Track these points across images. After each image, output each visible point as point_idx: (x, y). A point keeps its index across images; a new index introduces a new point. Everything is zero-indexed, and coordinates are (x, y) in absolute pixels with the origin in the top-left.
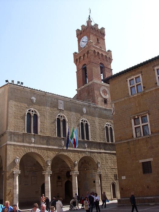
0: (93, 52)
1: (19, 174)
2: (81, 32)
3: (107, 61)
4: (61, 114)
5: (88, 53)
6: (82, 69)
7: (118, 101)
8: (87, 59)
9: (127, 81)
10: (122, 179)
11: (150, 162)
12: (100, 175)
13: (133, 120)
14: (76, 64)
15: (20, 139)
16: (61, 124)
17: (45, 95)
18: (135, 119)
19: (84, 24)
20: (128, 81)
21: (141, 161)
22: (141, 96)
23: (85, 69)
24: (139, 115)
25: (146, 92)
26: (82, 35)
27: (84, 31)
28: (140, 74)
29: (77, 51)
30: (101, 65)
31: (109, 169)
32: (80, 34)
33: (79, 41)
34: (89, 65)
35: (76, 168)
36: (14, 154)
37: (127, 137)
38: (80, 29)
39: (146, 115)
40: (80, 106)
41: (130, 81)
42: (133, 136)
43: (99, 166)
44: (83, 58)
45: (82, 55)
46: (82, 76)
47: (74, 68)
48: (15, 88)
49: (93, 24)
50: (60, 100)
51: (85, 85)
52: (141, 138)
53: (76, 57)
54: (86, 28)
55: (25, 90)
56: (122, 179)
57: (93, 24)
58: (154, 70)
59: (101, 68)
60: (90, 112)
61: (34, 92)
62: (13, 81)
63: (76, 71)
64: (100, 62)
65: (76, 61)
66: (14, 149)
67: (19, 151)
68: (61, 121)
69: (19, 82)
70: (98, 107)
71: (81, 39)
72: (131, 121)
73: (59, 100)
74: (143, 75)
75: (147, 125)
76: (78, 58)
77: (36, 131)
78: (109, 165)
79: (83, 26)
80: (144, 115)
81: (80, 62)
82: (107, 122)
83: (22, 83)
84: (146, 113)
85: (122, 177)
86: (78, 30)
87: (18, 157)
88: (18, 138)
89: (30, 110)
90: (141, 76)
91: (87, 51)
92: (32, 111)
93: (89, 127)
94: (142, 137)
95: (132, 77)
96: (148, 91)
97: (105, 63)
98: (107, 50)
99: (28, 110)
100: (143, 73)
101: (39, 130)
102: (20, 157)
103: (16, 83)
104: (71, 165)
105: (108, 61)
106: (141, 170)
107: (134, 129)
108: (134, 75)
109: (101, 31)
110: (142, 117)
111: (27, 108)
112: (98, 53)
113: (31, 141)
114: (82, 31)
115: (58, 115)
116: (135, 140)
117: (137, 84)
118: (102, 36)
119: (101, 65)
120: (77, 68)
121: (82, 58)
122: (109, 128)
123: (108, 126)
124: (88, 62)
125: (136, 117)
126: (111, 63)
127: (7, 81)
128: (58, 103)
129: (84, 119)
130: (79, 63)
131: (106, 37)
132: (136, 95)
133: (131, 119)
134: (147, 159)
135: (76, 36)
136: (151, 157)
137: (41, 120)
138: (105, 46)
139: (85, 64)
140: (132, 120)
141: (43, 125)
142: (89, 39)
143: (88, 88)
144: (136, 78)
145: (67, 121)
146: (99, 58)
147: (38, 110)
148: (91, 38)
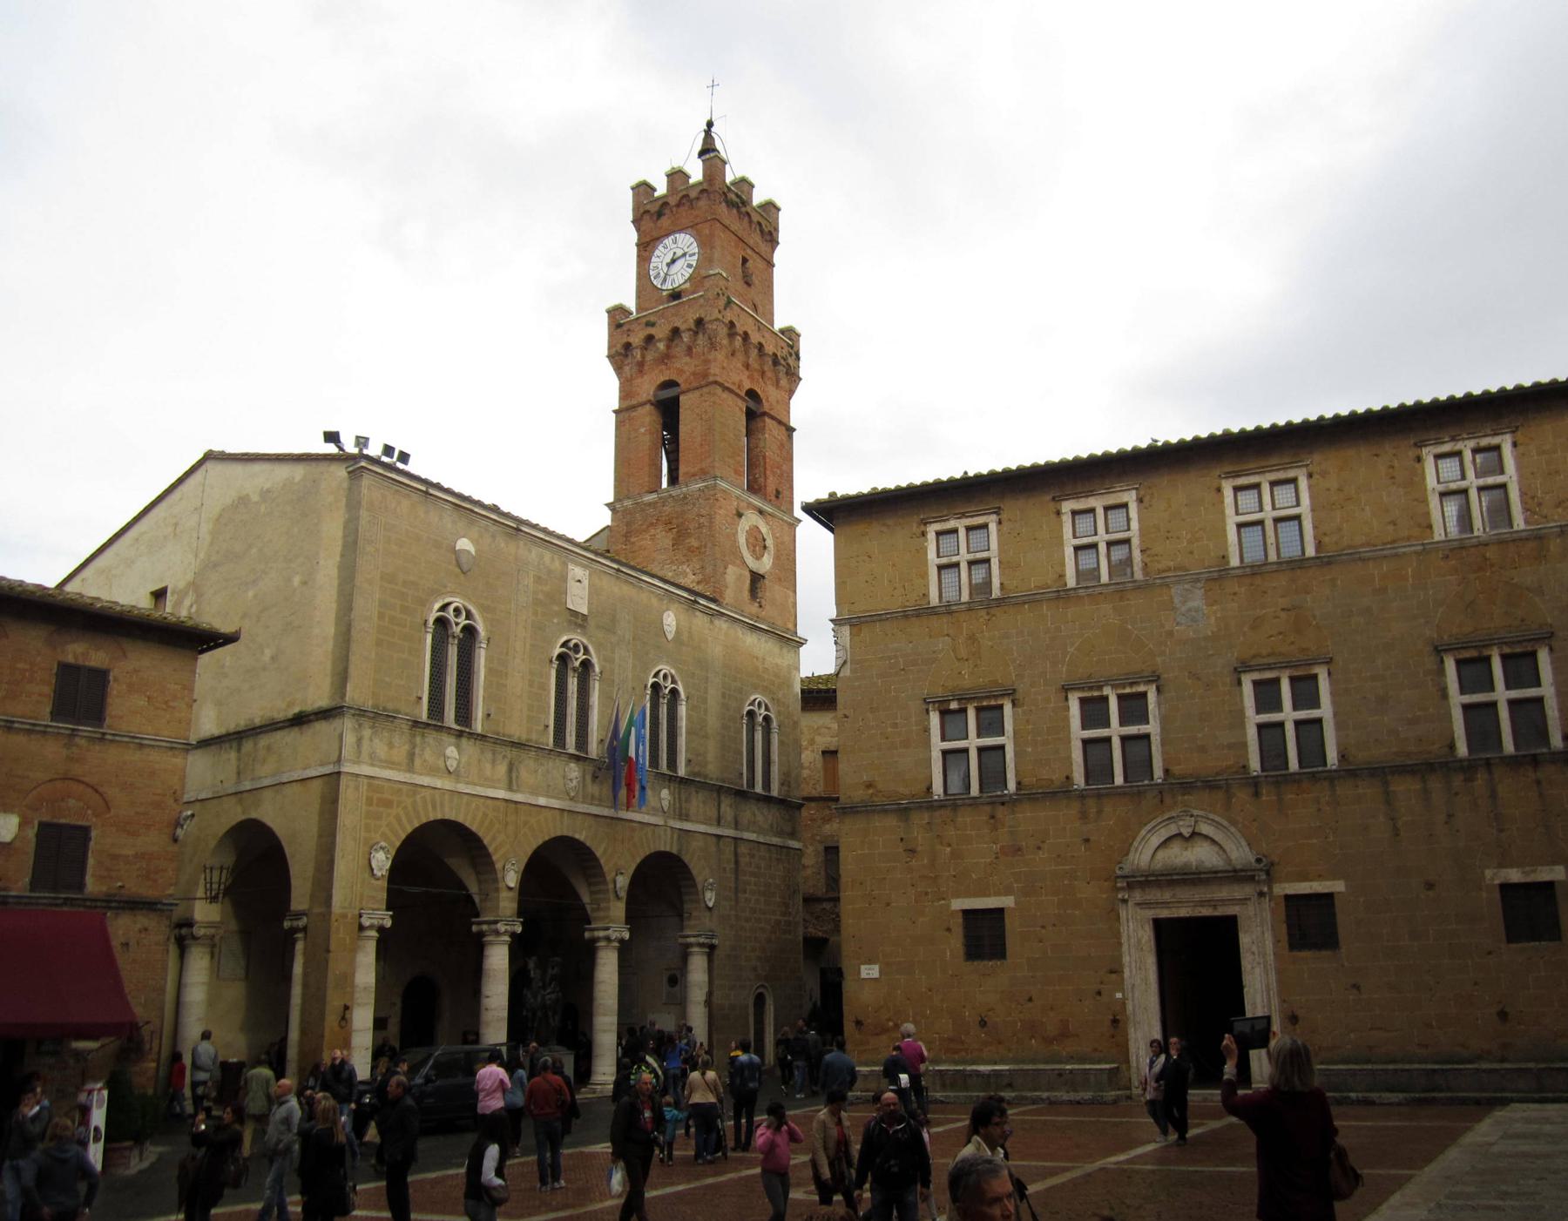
0: (723, 331)
1: (381, 929)
2: (666, 204)
3: (778, 381)
4: (576, 638)
9: (924, 534)
10: (864, 975)
11: (1000, 911)
12: (712, 947)
13: (935, 719)
14: (618, 369)
16: (573, 684)
18: (944, 713)
19: (687, 169)
20: (931, 536)
21: (959, 904)
23: (668, 411)
26: (665, 222)
27: (678, 205)
28: (994, 517)
29: (631, 304)
30: (752, 405)
31: (747, 920)
32: (656, 214)
33: (646, 248)
34: (697, 393)
35: (618, 909)
38: (661, 188)
40: (655, 601)
41: (939, 534)
42: (929, 788)
44: (668, 347)
45: (661, 332)
46: (647, 438)
47: (606, 388)
49: (729, 178)
50: (577, 564)
54: (693, 194)
56: (864, 975)
57: (729, 178)
59: (751, 415)
62: (362, 442)
63: (616, 407)
64: (747, 385)
65: (620, 355)
66: (369, 801)
68: (570, 674)
69: (388, 450)
71: (658, 239)
72: (928, 720)
73: (571, 566)
74: (1005, 523)
76: (637, 339)
77: (464, 714)
79: (676, 176)
80: (993, 703)
82: (756, 688)
83: (404, 457)
86: (643, 190)
87: (383, 844)
88: (391, 745)
89: (448, 604)
90: (993, 527)
91: (692, 316)
92: (457, 610)
93: (682, 710)
95: (951, 524)
98: (779, 323)
99: (437, 606)
100: (1004, 516)
101: (479, 712)
102: (391, 844)
103: (374, 450)
105: (784, 382)
106: (955, 943)
107: (936, 757)
108: (963, 515)
109: (764, 223)
112: (746, 336)
113: (442, 765)
114: (673, 201)
117: (971, 557)
118: (763, 247)
119: (752, 405)
121: (661, 346)
122: (760, 719)
123: (756, 708)
124: (694, 374)
125: (954, 706)
126: (791, 393)
127: (332, 437)
128: (564, 578)
129: (666, 669)
131: (778, 256)
133: (927, 711)
135: (630, 217)
136: (1007, 892)
137: (489, 659)
138: (771, 302)
139: (670, 384)
142: (706, 259)
143: (678, 509)
144: (969, 529)
145: (597, 669)
146: (747, 366)
147: (484, 609)
148: (717, 255)
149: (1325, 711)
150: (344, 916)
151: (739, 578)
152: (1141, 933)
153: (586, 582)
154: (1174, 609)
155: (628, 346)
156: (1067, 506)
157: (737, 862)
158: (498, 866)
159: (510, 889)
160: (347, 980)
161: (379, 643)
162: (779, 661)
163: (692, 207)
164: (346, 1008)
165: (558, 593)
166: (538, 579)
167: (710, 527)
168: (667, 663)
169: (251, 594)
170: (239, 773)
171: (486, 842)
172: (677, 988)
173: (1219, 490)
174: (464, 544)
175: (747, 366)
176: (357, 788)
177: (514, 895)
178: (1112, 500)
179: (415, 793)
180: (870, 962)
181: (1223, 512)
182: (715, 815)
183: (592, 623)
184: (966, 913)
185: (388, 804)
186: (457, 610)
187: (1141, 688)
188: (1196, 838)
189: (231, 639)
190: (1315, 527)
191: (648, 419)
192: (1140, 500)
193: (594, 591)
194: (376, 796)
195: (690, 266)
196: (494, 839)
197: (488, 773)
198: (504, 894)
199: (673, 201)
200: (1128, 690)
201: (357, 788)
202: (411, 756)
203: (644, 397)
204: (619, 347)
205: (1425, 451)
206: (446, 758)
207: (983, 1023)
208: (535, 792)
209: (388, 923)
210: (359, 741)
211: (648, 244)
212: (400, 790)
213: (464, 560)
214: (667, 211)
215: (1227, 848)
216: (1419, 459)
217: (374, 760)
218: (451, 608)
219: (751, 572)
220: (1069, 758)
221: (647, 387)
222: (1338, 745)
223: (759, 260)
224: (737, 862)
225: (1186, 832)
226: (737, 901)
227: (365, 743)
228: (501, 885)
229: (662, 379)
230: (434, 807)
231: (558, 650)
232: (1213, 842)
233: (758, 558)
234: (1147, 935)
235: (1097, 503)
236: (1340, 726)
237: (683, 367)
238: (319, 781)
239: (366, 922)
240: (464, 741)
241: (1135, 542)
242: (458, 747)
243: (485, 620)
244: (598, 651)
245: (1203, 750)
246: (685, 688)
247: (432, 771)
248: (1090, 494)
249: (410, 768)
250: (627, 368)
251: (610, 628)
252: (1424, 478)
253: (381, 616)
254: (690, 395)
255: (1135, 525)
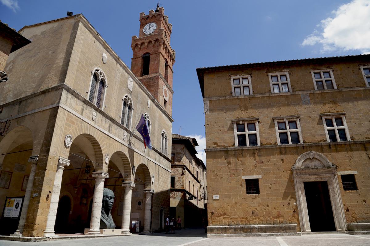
1: (66, 167)
4: (129, 96)
5: (157, 40)
6: (142, 57)
7: (215, 99)
8: (153, 48)
14: (134, 50)
15: (78, 106)
17: (117, 60)
22: (248, 99)
24: (245, 121)
25: (257, 96)
26: (148, 20)
27: (152, 17)
28: (250, 76)
33: (142, 25)
34: (155, 55)
36: (66, 128)
37: (225, 145)
39: (254, 122)
41: (234, 79)
42: (234, 144)
43: (153, 182)
44: (148, 45)
45: (147, 41)
48: (87, 26)
51: (144, 77)
52: (246, 148)
53: (136, 41)
55: (98, 38)
58: (268, 75)
60: (153, 109)
61: (108, 49)
63: (132, 58)
66: (67, 120)
67: (74, 126)
70: (159, 106)
72: (233, 126)
74: (253, 77)
75: (255, 134)
78: (160, 183)
80: (252, 122)
81: (140, 48)
84: (255, 120)
85: (214, 196)
87: (71, 135)
88: (77, 104)
90: (250, 78)
94: (248, 147)
95: (238, 77)
96: (259, 96)
97: (170, 63)
99: (96, 69)
104: (125, 172)
105: (172, 61)
110: (248, 124)
111: (95, 64)
114: (150, 16)
115: (126, 95)
116: (237, 150)
118: (169, 33)
120: (134, 55)
121: (146, 44)
122: (165, 136)
123: (164, 133)
124: (154, 51)
125: (241, 123)
129: (148, 114)
130: (138, 50)
132: (243, 97)
133: (233, 124)
134: (254, 175)
136: (260, 174)
140: (234, 124)
141: (109, 99)
145: (133, 107)
147: (108, 76)
149: (346, 126)
150: (54, 157)
151: (162, 99)
152: (301, 185)
153: (132, 83)
154: (302, 100)
155: (137, 45)
156: (270, 74)
157: (159, 172)
158: (104, 155)
159: (106, 163)
160: (52, 181)
161: (77, 71)
162: (169, 123)
163: (155, 17)
164: (50, 192)
165: (126, 82)
166: (122, 76)
167: (157, 85)
168: (148, 113)
169: (33, 60)
170: (18, 112)
171: (101, 146)
172: (141, 206)
173: (310, 73)
174: (104, 55)
175: (166, 53)
176: (64, 114)
177: (107, 165)
178: (282, 73)
179: (82, 123)
180: (216, 194)
181: (312, 78)
182: (155, 158)
183: (133, 94)
184: (246, 180)
185: (73, 123)
186: (101, 74)
187: (295, 120)
188: (314, 159)
189: (30, 42)
190: (336, 83)
191: (140, 62)
192: (290, 74)
193: (134, 86)
194: (70, 119)
195: (154, 29)
196: (103, 146)
197: (104, 125)
198: (104, 164)
199: (150, 16)
200: (291, 120)
201: (64, 114)
202: (83, 110)
203: (140, 56)
204: (134, 45)
205: (361, 67)
206: (93, 115)
207: (253, 213)
208: (115, 135)
209: (68, 164)
210: (67, 98)
211: (143, 25)
212: (77, 120)
213: (104, 59)
214: (149, 19)
215: (323, 162)
216: (360, 69)
217: (70, 106)
218: (99, 71)
219: (165, 99)
220: (276, 137)
221: (141, 54)
222: (350, 135)
223: (168, 34)
224: (159, 172)
225: (311, 157)
226: (158, 183)
227: (69, 100)
228: (104, 161)
229: (145, 52)
230: (87, 129)
231: (124, 97)
232: (319, 160)
233: (166, 97)
234: (302, 186)
235: (278, 74)
236: (350, 130)
237: (151, 50)
238: (50, 110)
239: (61, 162)
240: (98, 113)
241: (289, 84)
242: (96, 113)
243: (108, 80)
244: (133, 102)
245: (313, 136)
246: (151, 121)
247: (88, 118)
248: (276, 71)
249: (82, 114)
250: (136, 50)
251: (137, 98)
252: (361, 73)
253: (79, 63)
254: (153, 55)
255: (289, 79)
